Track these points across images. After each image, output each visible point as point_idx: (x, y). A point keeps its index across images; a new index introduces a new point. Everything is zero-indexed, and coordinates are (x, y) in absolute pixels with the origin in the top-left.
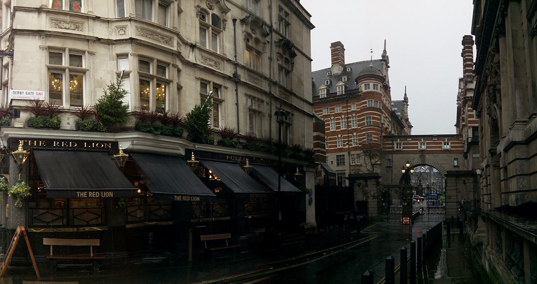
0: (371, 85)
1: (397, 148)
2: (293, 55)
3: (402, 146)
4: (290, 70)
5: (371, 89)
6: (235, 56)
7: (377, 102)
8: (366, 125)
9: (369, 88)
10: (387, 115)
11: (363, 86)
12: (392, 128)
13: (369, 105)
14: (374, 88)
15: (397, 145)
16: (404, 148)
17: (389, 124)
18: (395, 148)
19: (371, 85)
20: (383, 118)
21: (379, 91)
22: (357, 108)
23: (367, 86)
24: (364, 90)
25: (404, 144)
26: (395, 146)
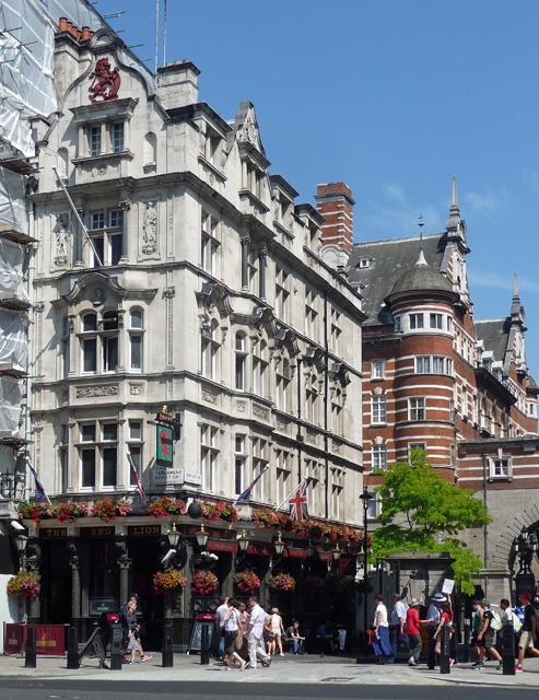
0: (427, 315)
1: (498, 472)
2: (345, 383)
3: (511, 467)
4: (341, 405)
5: (427, 328)
6: (299, 411)
7: (442, 359)
8: (409, 419)
9: (421, 325)
10: (465, 383)
11: (406, 318)
12: (480, 411)
13: (420, 369)
14: (433, 326)
15: (497, 464)
16: (516, 472)
17: (473, 404)
18: (493, 474)
19: (427, 315)
20: (456, 394)
21: (444, 331)
22: (388, 375)
23: (416, 320)
24: (407, 329)
25: (516, 462)
26: (493, 467)
